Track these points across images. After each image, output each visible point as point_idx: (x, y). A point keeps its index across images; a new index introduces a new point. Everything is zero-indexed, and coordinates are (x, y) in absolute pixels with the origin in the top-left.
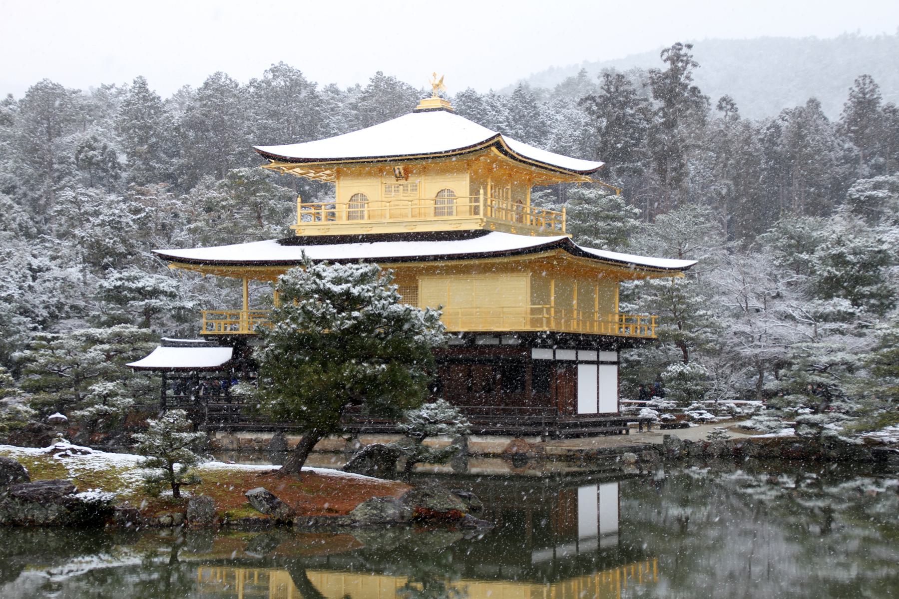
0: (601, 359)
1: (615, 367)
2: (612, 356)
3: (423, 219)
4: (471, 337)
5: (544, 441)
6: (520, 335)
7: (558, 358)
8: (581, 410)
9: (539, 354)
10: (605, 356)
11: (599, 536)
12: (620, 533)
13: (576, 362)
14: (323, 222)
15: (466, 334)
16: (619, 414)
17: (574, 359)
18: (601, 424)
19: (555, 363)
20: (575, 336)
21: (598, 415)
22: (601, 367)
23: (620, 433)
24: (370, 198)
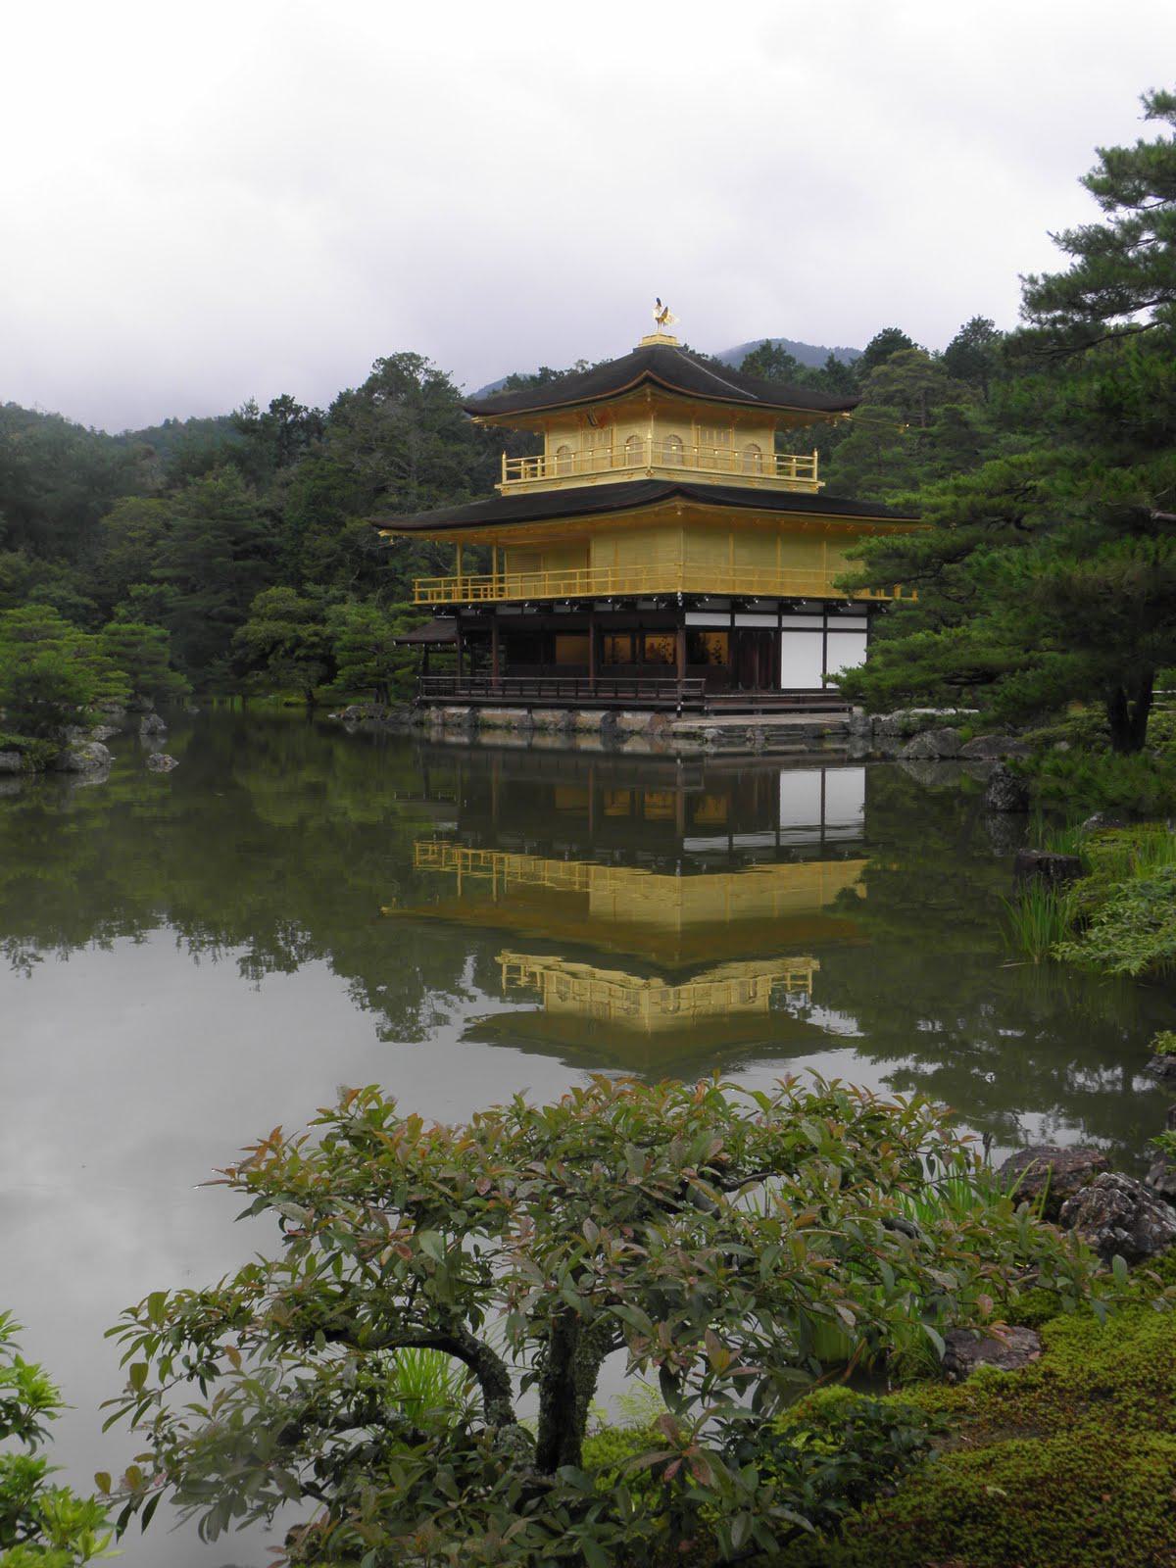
1: (865, 636)
2: (862, 623)
4: (629, 603)
5: (679, 715)
6: (662, 597)
7: (738, 623)
8: (785, 685)
9: (692, 620)
10: (833, 622)
11: (823, 827)
15: (616, 599)
16: (824, 689)
17: (776, 625)
19: (731, 630)
20: (749, 599)
23: (843, 710)
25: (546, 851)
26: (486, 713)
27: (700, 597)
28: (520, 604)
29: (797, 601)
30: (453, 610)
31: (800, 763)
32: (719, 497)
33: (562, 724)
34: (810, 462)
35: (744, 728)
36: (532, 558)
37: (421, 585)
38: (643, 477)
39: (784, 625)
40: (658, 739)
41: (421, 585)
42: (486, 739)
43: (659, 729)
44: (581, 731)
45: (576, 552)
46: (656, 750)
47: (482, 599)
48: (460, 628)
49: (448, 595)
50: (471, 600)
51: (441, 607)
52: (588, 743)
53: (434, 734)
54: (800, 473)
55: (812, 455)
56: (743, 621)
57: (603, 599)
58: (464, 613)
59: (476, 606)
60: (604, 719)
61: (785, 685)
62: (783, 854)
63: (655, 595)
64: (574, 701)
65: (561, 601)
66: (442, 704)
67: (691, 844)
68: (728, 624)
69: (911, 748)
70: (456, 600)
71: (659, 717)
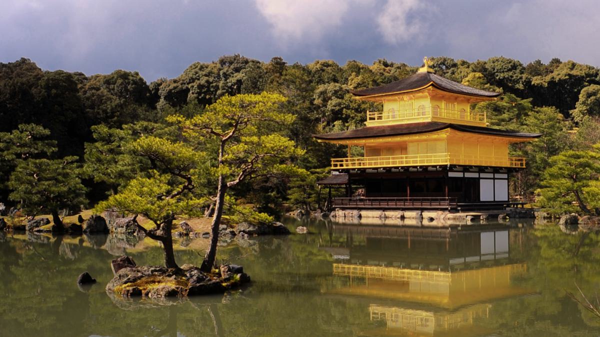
0: (496, 177)
1: (506, 181)
2: (506, 176)
3: (413, 117)
4: (425, 168)
6: (441, 166)
7: (466, 176)
8: (481, 200)
9: (451, 174)
10: (497, 176)
11: (495, 254)
12: (509, 252)
13: (479, 178)
14: (376, 120)
15: (421, 167)
17: (478, 176)
18: (495, 206)
19: (463, 179)
21: (494, 201)
22: (496, 180)
23: (502, 209)
24: (396, 109)
25: (389, 265)
26: (363, 213)
27: (455, 166)
28: (377, 169)
29: (486, 167)
30: (347, 171)
31: (485, 228)
32: (495, 133)
33: (399, 216)
34: (484, 115)
35: (480, 215)
36: (375, 151)
37: (334, 161)
38: (429, 120)
39: (481, 176)
40: (442, 221)
41: (334, 161)
42: (363, 221)
43: (442, 217)
44: (407, 218)
45: (402, 148)
46: (440, 225)
47: (362, 167)
48: (349, 178)
49: (347, 166)
50: (357, 167)
51: (343, 170)
52: (407, 222)
53: (341, 220)
54: (480, 120)
55: (483, 112)
56: (467, 175)
57: (416, 167)
58: (351, 171)
59: (359, 169)
60: (417, 214)
61: (481, 200)
62: (482, 265)
63: (438, 165)
64: (403, 207)
65: (397, 168)
66: (343, 209)
67: (451, 262)
68: (462, 176)
69: (562, 221)
70: (350, 167)
71: (440, 212)
